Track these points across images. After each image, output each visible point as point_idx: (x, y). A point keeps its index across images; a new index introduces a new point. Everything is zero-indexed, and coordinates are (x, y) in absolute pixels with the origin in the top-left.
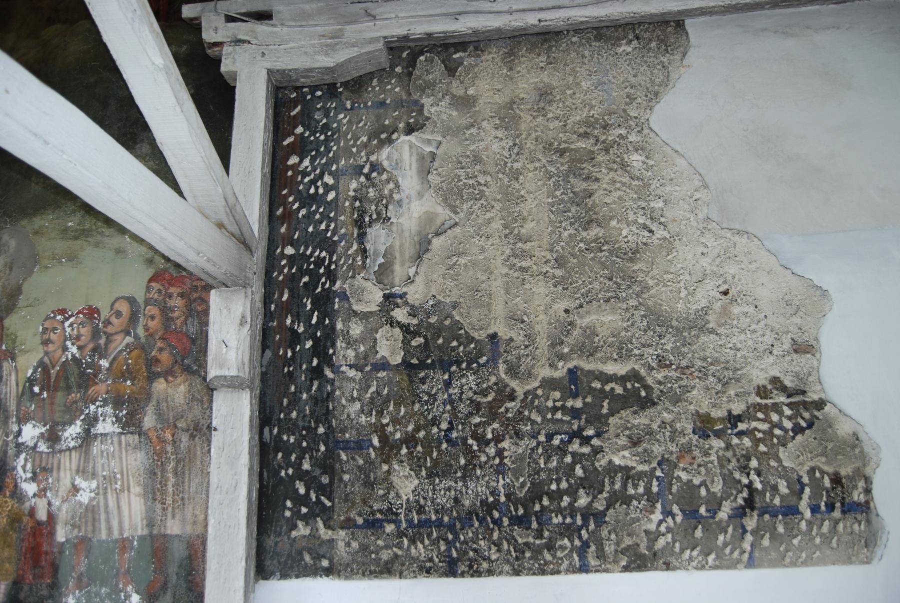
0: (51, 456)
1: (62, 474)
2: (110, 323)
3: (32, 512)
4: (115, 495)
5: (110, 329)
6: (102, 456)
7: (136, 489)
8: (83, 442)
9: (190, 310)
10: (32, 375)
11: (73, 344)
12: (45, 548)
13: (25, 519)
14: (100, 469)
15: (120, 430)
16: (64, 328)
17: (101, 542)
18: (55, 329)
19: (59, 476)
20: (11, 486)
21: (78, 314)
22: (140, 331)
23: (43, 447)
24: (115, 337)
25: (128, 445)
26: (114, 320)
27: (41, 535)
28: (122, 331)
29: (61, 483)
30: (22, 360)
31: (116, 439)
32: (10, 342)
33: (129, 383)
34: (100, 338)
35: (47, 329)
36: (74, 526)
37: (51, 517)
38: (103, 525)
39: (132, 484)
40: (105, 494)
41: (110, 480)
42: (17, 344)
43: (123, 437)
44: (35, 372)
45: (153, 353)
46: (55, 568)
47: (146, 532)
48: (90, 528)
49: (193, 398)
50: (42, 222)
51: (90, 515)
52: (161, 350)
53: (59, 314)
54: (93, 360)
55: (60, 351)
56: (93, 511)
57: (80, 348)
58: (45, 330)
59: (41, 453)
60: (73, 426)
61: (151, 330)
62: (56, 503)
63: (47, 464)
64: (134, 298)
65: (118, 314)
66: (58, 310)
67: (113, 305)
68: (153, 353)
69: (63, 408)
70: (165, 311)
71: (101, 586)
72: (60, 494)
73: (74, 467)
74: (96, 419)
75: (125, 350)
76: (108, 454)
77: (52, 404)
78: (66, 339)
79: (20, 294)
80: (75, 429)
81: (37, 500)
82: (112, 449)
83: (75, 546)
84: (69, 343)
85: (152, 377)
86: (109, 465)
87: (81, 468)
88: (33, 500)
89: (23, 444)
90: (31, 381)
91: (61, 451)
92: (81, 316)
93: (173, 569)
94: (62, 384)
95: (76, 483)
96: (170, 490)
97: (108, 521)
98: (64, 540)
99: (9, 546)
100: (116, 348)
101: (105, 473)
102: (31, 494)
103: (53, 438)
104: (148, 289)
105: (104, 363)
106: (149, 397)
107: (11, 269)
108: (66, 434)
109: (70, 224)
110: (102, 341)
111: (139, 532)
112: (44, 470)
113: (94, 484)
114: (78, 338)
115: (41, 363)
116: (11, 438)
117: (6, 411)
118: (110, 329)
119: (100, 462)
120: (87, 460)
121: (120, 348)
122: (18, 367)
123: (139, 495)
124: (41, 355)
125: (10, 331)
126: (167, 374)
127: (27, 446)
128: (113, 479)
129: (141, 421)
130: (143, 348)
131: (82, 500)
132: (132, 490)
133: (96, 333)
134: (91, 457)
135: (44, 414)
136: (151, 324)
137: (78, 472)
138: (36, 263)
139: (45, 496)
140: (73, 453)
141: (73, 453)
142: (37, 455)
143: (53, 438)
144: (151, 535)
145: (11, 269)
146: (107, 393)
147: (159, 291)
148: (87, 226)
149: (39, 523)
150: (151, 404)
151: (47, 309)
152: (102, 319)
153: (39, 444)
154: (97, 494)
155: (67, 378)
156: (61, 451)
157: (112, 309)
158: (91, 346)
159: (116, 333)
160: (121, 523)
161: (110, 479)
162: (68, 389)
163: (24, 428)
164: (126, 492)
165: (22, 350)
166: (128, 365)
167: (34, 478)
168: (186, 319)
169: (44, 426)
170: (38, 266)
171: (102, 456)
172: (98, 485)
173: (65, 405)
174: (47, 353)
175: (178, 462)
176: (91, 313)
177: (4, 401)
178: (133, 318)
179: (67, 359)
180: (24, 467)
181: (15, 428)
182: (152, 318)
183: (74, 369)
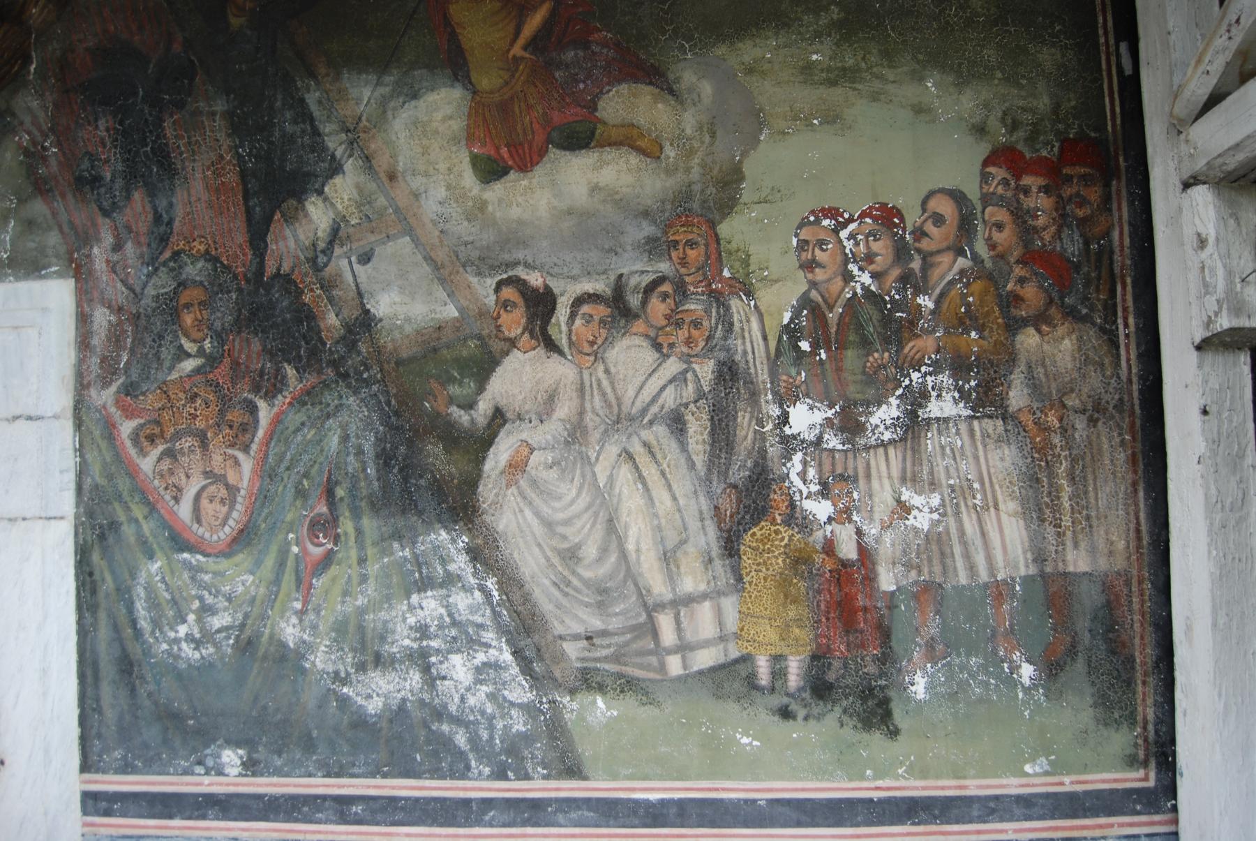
0: (850, 455)
1: (875, 484)
2: (925, 234)
3: (829, 547)
4: (974, 516)
5: (925, 244)
6: (943, 454)
7: (1009, 506)
8: (906, 432)
9: (1063, 216)
10: (792, 320)
11: (861, 269)
12: (861, 601)
13: (819, 559)
14: (943, 476)
15: (969, 412)
16: (840, 241)
17: (959, 590)
18: (821, 243)
19: (870, 489)
20: (783, 506)
21: (863, 215)
22: (981, 248)
23: (833, 441)
24: (938, 259)
25: (986, 435)
26: (930, 228)
27: (853, 582)
28: (948, 248)
29: (876, 499)
30: (766, 297)
31: (963, 427)
32: (737, 265)
33: (973, 334)
34: (911, 259)
35: (806, 242)
36: (908, 566)
37: (863, 550)
38: (960, 563)
39: (1000, 497)
40: (957, 514)
41: (963, 493)
42: (751, 269)
43: (976, 423)
44: (796, 314)
45: (1010, 287)
46: (885, 634)
47: (1032, 570)
48: (937, 569)
49: (1087, 361)
50: (758, 52)
51: (934, 547)
52: (1022, 281)
53: (826, 217)
54: (905, 297)
55: (839, 282)
56: (939, 541)
57: (874, 276)
58: (803, 244)
59: (833, 451)
60: (884, 407)
61: (1000, 249)
62: (872, 530)
63: (846, 469)
64: (961, 192)
65: (938, 219)
66: (823, 210)
67: (924, 203)
68: (1010, 287)
69: (859, 377)
70: (1020, 216)
71: (968, 655)
72: (877, 516)
73: (896, 472)
74: (925, 395)
75: (960, 280)
76: (952, 450)
77: (839, 370)
78: (846, 261)
79: (742, 179)
80: (887, 413)
81: (837, 528)
82: (959, 443)
83: (916, 597)
84: (853, 268)
85: (1013, 326)
86: (957, 469)
87: (909, 475)
88: (829, 528)
89: (794, 437)
90: (792, 332)
91: (868, 448)
92: (868, 220)
93: (1083, 624)
94: (852, 337)
95: (903, 498)
96: (1067, 505)
97: (967, 556)
98: (893, 588)
99: (794, 601)
100: (942, 277)
101: (952, 482)
102: (823, 518)
103: (850, 425)
104: (985, 178)
105: (926, 302)
106: (1012, 359)
107: (713, 135)
108: (874, 420)
109: (815, 57)
110: (916, 265)
111: (1023, 572)
112: (843, 478)
113: (935, 500)
114: (870, 258)
115: (805, 301)
116: (769, 427)
117: (750, 382)
118: (925, 244)
119: (941, 464)
120: (917, 461)
121: (949, 277)
122: (763, 309)
123: (1015, 514)
124: (805, 287)
125: (734, 246)
126: (1039, 320)
127: (803, 441)
128: (967, 491)
129: (1003, 398)
130: (990, 277)
131: (919, 526)
132: (1001, 506)
133: (901, 252)
134: (924, 457)
135: (826, 386)
136: (997, 236)
137: (903, 480)
138: (761, 125)
139: (850, 520)
140: (891, 451)
141: (891, 451)
142: (825, 455)
143: (850, 425)
144: (1043, 575)
145: (713, 135)
146: (938, 351)
147: (1005, 182)
148: (850, 62)
149: (845, 564)
150: (1017, 370)
151: (802, 206)
152: (909, 228)
153: (826, 436)
154: (944, 515)
155: (860, 327)
156: (868, 448)
157: (924, 210)
158: (896, 273)
159: (939, 252)
160: (989, 558)
161: (962, 491)
162: (865, 344)
163: (791, 410)
164: (992, 509)
165: (764, 279)
166: (968, 305)
167: (825, 491)
168: (1059, 231)
169: (831, 407)
170: (766, 131)
171: (943, 454)
172: (943, 500)
173: (864, 373)
174: (813, 284)
175: (1074, 461)
176: (887, 216)
177: (742, 365)
178: (966, 225)
179: (855, 294)
180: (803, 475)
181: (775, 411)
182: (1000, 226)
183: (869, 311)
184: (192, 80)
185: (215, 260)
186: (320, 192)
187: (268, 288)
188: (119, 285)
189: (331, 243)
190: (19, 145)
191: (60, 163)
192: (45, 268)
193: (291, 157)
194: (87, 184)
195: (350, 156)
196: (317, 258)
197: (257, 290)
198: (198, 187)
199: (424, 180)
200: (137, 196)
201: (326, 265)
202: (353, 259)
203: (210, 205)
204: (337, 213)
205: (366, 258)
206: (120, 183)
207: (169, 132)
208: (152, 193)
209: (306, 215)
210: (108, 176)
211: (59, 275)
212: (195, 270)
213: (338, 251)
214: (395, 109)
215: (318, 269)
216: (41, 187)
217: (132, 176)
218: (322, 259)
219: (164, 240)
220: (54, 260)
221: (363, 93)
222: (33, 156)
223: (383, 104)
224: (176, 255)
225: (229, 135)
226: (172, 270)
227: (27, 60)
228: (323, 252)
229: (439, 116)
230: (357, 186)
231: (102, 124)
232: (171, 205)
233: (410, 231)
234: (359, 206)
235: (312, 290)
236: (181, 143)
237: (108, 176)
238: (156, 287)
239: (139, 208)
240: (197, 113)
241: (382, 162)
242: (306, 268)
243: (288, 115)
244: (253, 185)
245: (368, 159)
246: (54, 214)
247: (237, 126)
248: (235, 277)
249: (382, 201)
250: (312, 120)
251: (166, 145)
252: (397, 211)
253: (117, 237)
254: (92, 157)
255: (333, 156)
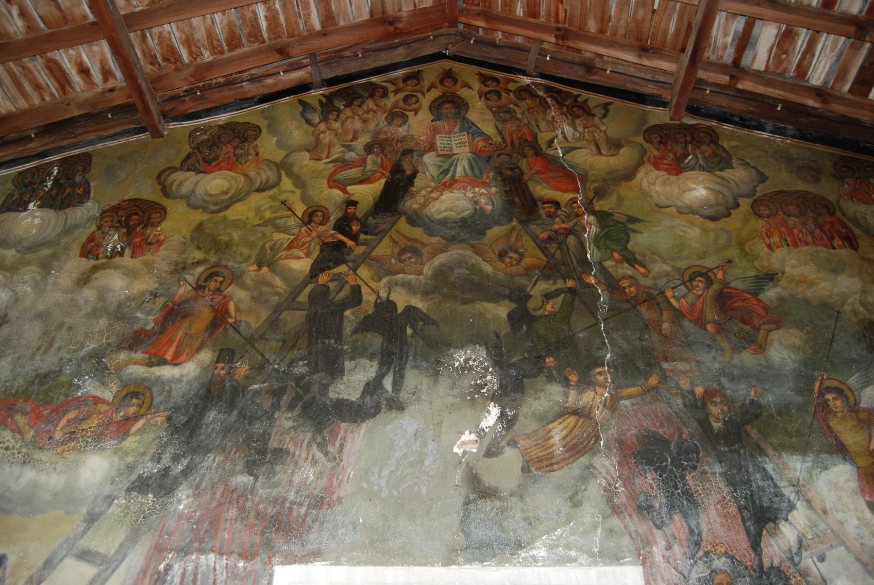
184: (698, 454)
185: (732, 558)
186: (786, 520)
187: (768, 575)
188: (673, 571)
189: (799, 549)
190: (600, 485)
191: (627, 496)
192: (622, 558)
193: (765, 499)
194: (645, 509)
195: (799, 500)
196: (794, 556)
197: (761, 577)
198: (713, 513)
199: (843, 514)
200: (676, 517)
201: (800, 562)
202: (815, 559)
203: (722, 525)
204: (799, 532)
205: (822, 559)
206: (664, 510)
207: (690, 482)
208: (685, 516)
209: (781, 533)
210: (657, 505)
211: (632, 563)
212: (720, 563)
213: (804, 554)
214: (817, 475)
215: (796, 565)
216: (616, 511)
217: (672, 507)
218: (796, 559)
219: (698, 544)
220: (628, 554)
221: (797, 465)
222: (609, 493)
223: (810, 471)
224: (707, 554)
225: (727, 486)
226: (706, 562)
227: (598, 438)
228: (796, 554)
229: (842, 479)
230: (807, 517)
231: (648, 475)
232: (699, 524)
233: (843, 543)
234: (811, 528)
235: (795, 577)
236: (699, 488)
237: (657, 505)
238: (697, 573)
239: (679, 525)
240: (704, 472)
241: (817, 503)
242: (788, 563)
243: (758, 476)
244: (746, 514)
245: (808, 501)
246: (626, 527)
247: (731, 483)
248: (746, 568)
249: (822, 526)
250: (772, 479)
251: (690, 489)
252: (833, 531)
253: (667, 541)
254: (646, 494)
255: (789, 500)
